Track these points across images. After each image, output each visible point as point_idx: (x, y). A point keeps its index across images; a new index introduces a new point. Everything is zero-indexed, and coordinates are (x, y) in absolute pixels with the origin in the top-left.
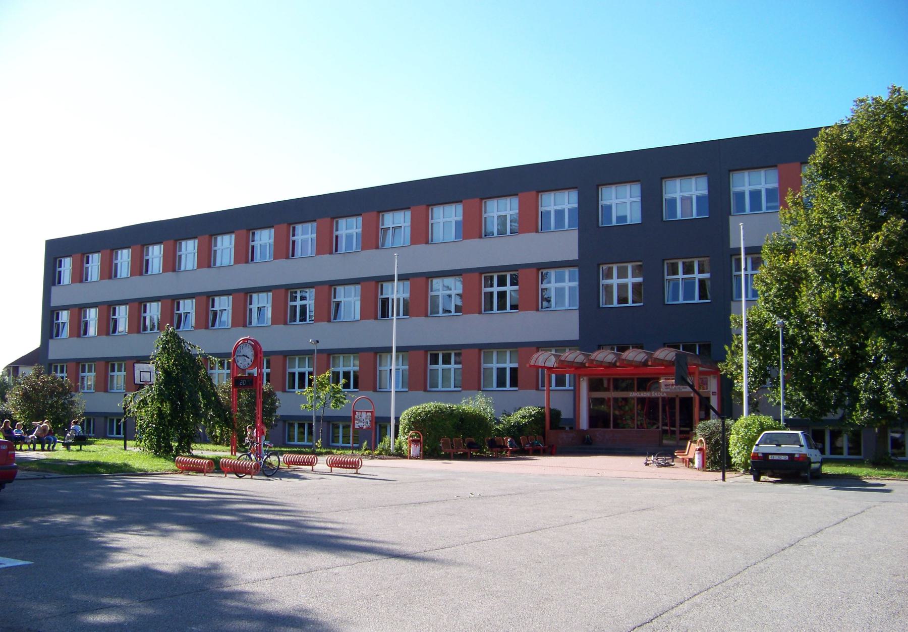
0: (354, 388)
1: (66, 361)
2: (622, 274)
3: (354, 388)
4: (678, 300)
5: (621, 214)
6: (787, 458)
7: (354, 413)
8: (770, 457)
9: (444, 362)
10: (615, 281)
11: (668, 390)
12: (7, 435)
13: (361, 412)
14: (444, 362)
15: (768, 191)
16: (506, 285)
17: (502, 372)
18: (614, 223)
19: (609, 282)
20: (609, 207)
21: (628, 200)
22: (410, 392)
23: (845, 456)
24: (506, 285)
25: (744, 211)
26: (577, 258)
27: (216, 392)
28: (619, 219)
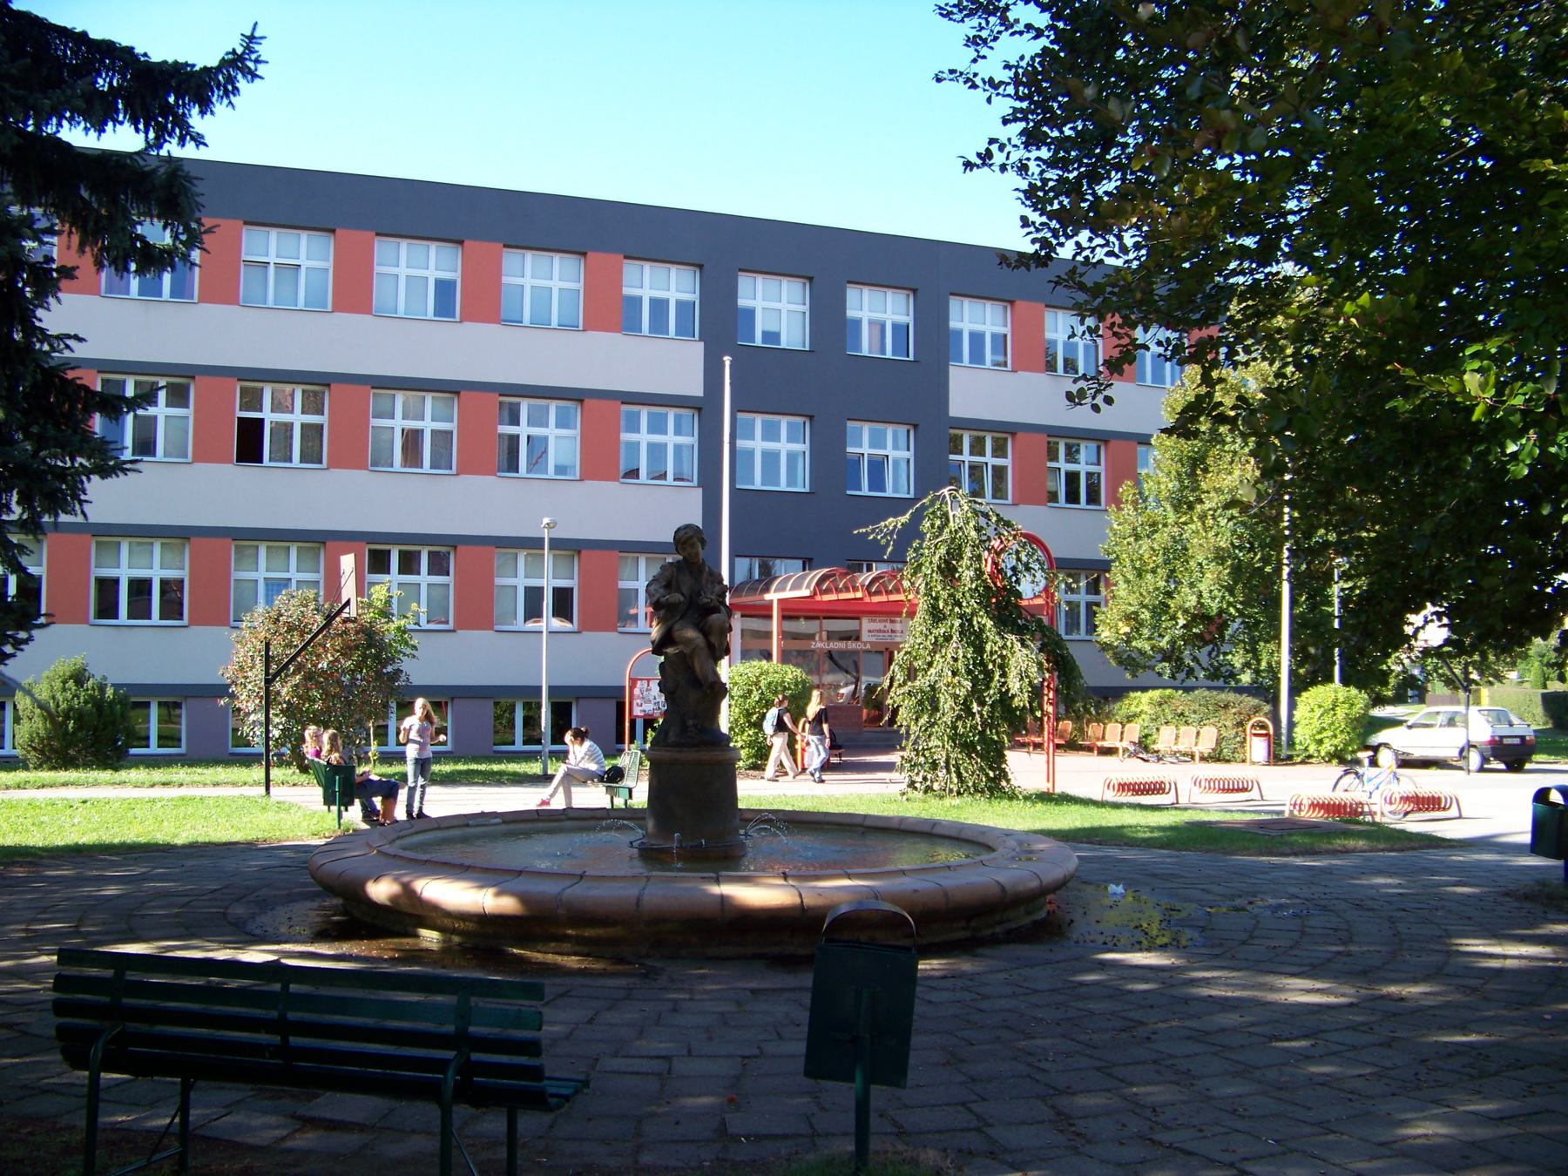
0: (161, 618)
1: (455, 542)
2: (771, 433)
3: (161, 618)
4: (884, 491)
5: (772, 328)
6: (1517, 741)
7: (633, 682)
8: (1506, 741)
9: (404, 570)
10: (644, 437)
11: (874, 639)
12: (716, 755)
13: (648, 680)
14: (404, 570)
15: (679, 304)
16: (665, 433)
17: (534, 595)
18: (758, 342)
19: (632, 437)
20: (751, 313)
21: (784, 306)
22: (460, 632)
23: (519, 746)
24: (665, 433)
25: (160, 296)
26: (701, 394)
27: (1513, 651)
28: (768, 336)
